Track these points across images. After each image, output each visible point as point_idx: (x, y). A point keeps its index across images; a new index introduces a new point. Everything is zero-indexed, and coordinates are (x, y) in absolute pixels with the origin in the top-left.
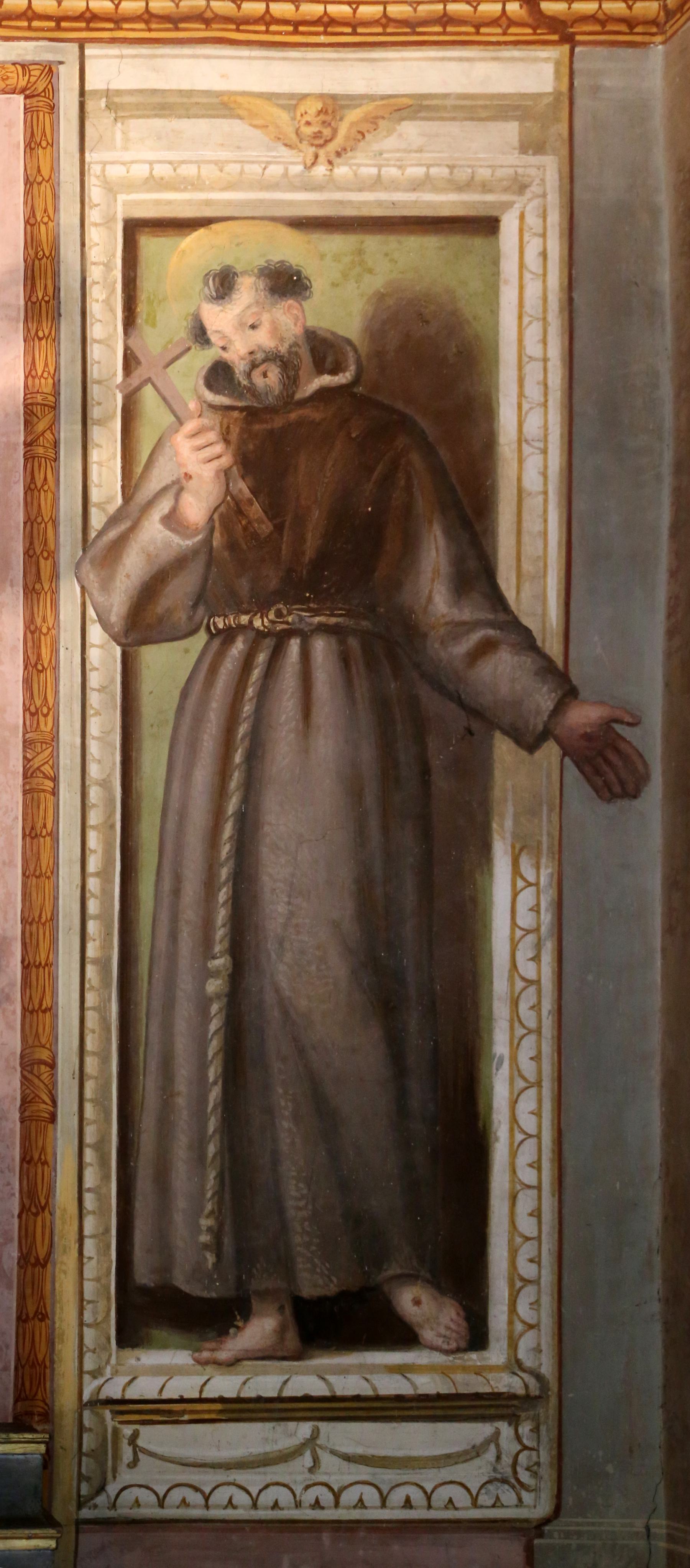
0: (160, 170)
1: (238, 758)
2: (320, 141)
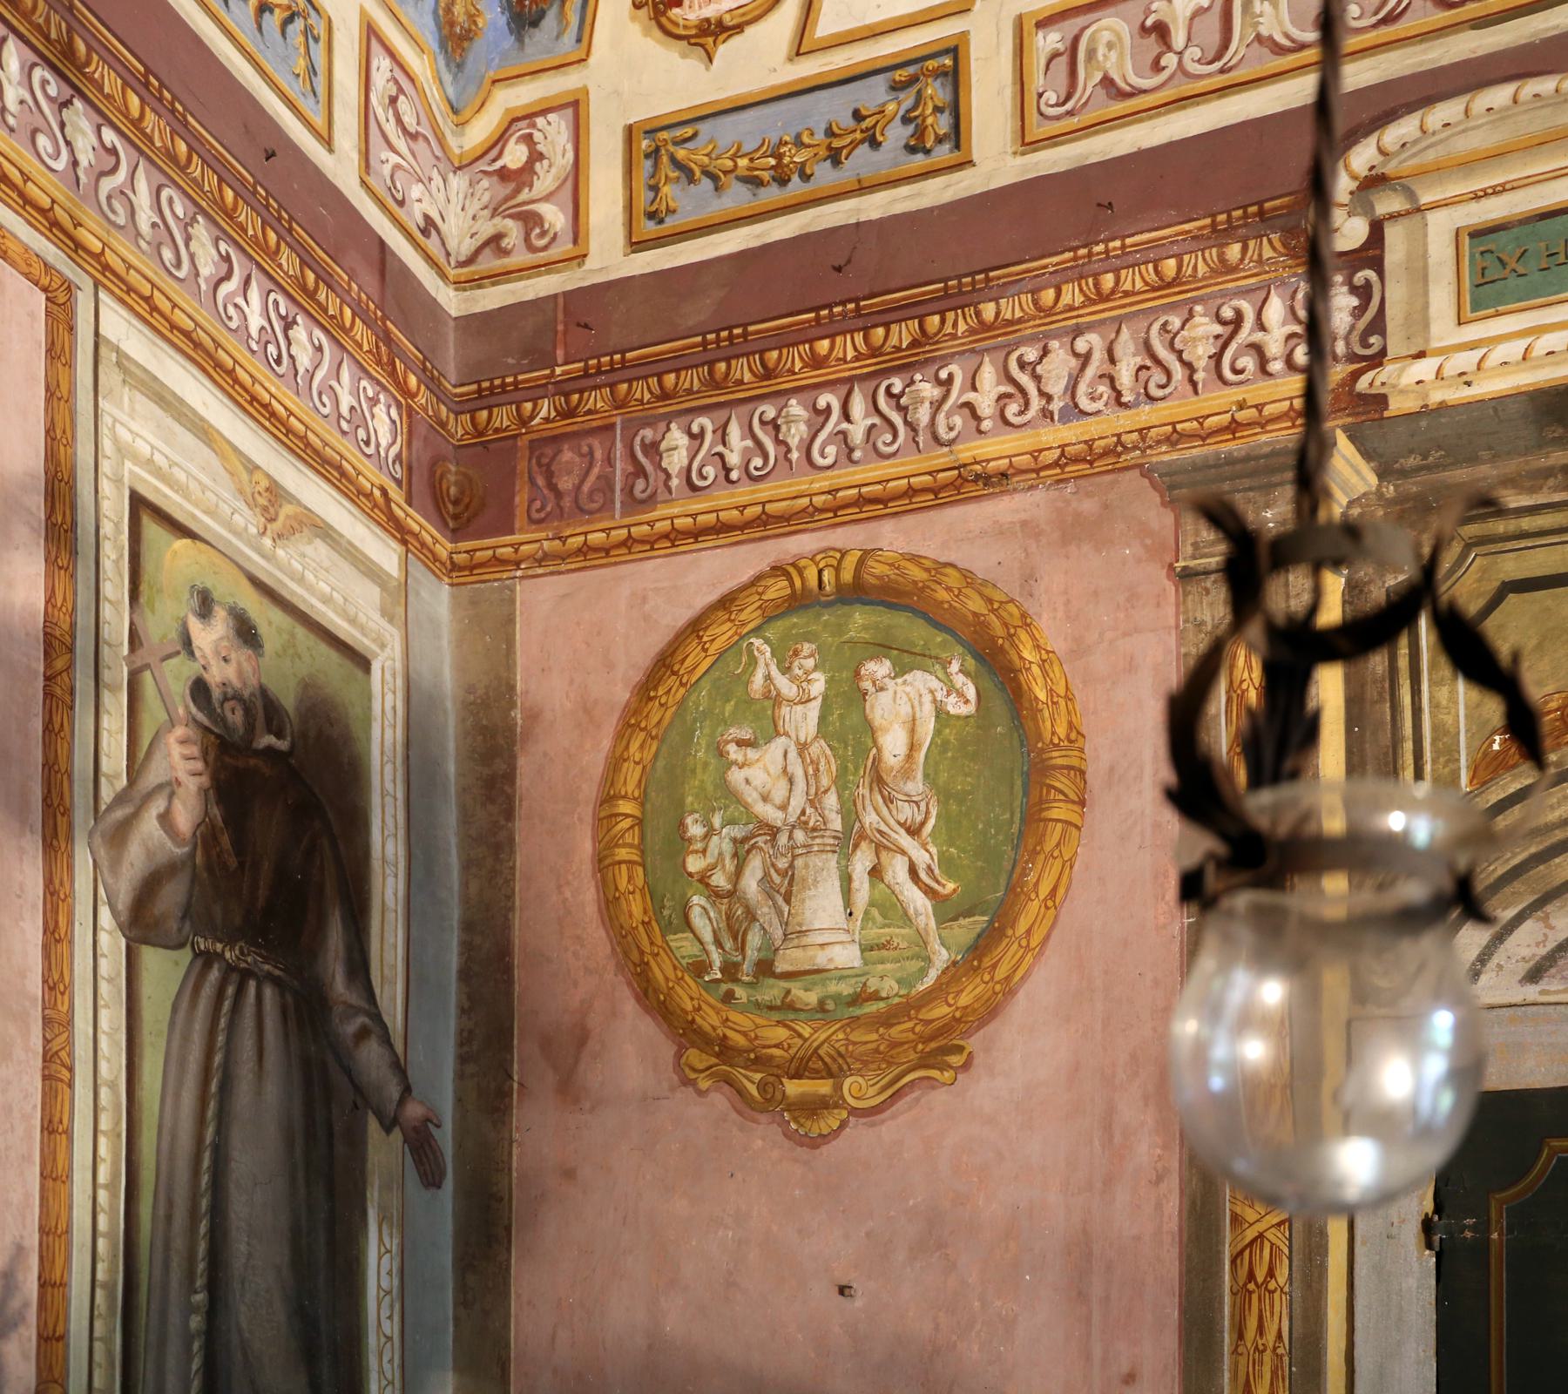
1: (214, 1087)
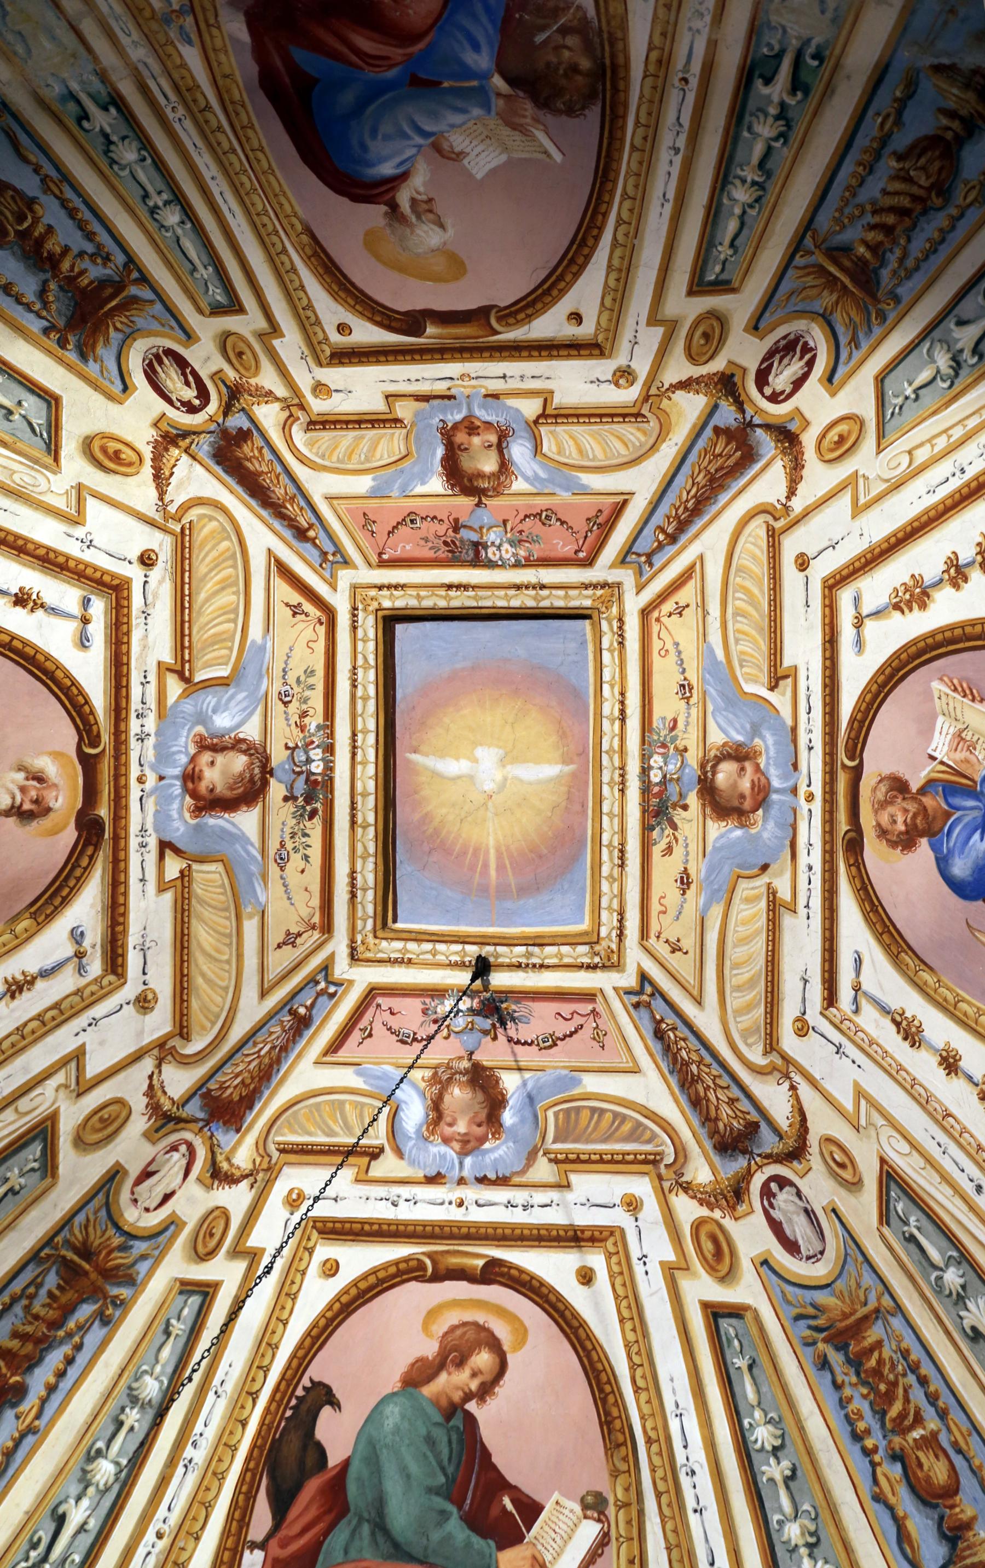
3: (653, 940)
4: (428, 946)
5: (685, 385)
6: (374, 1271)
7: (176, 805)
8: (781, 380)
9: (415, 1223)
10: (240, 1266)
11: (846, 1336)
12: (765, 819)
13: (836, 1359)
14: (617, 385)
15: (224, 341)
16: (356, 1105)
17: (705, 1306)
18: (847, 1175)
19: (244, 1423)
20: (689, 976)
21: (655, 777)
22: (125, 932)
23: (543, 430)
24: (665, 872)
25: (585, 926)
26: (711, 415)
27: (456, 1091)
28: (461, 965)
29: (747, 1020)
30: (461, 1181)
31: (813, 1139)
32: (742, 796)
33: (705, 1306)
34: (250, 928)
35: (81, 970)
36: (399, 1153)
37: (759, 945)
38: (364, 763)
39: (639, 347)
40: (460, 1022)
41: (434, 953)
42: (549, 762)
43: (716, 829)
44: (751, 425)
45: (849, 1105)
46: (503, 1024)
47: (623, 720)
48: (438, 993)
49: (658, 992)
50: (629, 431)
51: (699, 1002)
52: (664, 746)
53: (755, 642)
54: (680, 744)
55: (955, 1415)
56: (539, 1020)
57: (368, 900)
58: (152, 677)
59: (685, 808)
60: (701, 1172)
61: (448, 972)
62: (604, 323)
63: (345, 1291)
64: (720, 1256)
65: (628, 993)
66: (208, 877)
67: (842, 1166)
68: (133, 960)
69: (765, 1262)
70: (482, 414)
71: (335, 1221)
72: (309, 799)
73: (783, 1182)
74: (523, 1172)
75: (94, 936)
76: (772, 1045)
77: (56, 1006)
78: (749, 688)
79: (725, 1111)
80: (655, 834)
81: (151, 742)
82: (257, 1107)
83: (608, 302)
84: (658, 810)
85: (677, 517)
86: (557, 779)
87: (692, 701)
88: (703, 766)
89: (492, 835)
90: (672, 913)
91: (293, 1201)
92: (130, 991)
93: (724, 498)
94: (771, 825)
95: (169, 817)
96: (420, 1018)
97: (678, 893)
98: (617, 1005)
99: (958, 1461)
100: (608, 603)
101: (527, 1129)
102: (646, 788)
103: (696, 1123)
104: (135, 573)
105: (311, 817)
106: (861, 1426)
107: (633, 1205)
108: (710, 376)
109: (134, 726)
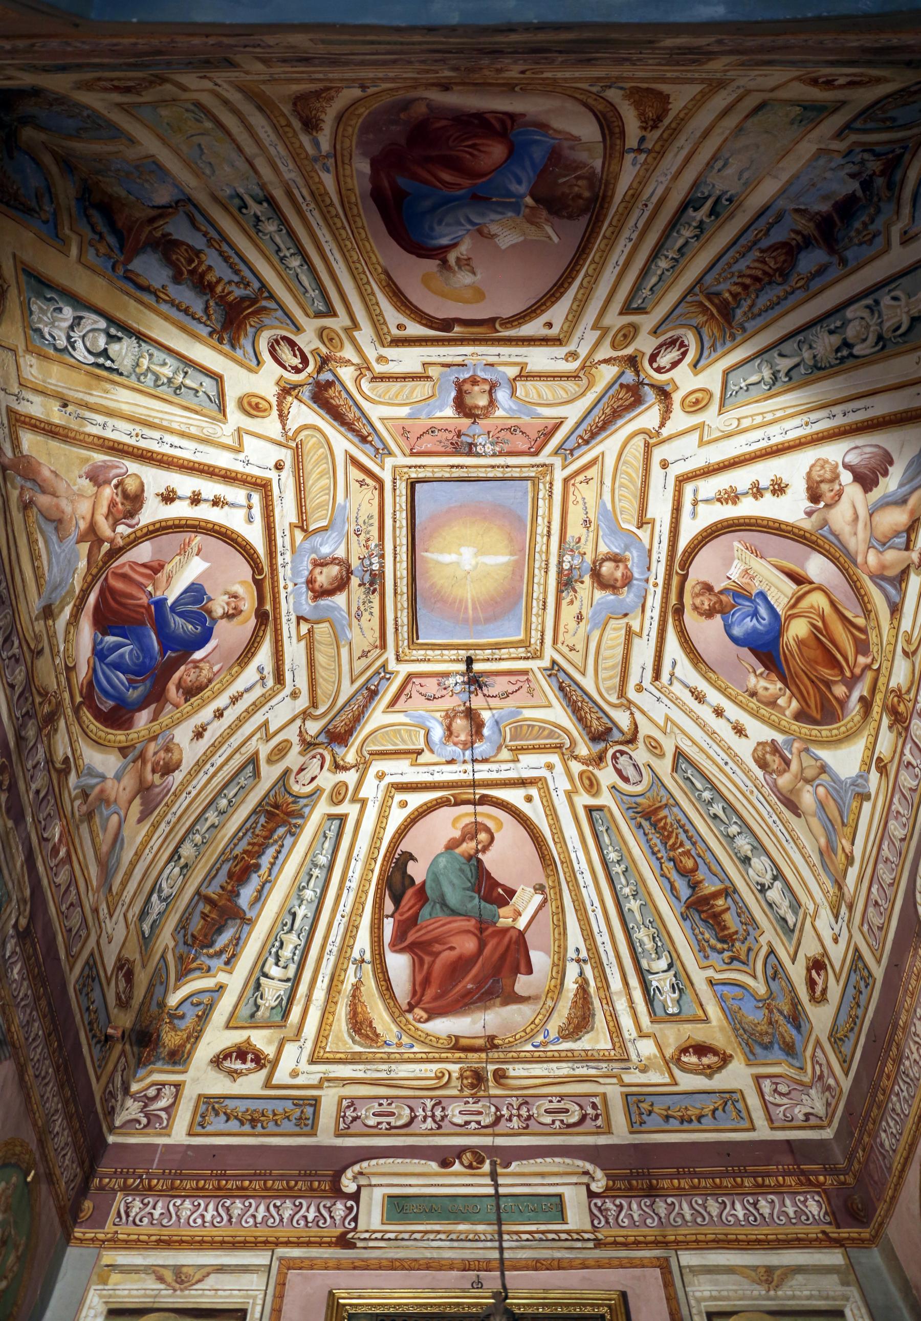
0: (714, 1293)
2: (769, 1282)
3: (559, 645)
4: (439, 652)
5: (606, 361)
6: (425, 804)
7: (304, 597)
8: (664, 360)
9: (444, 782)
10: (357, 806)
11: (651, 816)
12: (628, 592)
13: (646, 824)
14: (567, 360)
15: (321, 333)
16: (407, 731)
17: (586, 807)
18: (657, 751)
19: (372, 871)
20: (580, 664)
21: (566, 566)
22: (283, 663)
23: (518, 384)
24: (569, 614)
25: (522, 637)
26: (619, 377)
27: (459, 721)
28: (458, 661)
29: (609, 683)
30: (465, 762)
31: (640, 736)
32: (616, 580)
33: (586, 807)
34: (344, 652)
35: (264, 685)
36: (432, 751)
37: (620, 650)
38: (401, 562)
39: (584, 341)
40: (458, 688)
41: (442, 655)
42: (502, 554)
43: (599, 594)
44: (642, 383)
45: (661, 723)
46: (481, 688)
47: (549, 536)
48: (446, 675)
49: (561, 669)
50: (571, 386)
51: (584, 674)
52: (572, 551)
53: (631, 503)
54: (582, 551)
55: (700, 843)
56: (500, 685)
57: (404, 631)
58: (287, 532)
59: (582, 582)
60: (583, 750)
61: (450, 664)
62: (565, 328)
63: (413, 813)
64: (592, 786)
65: (545, 669)
66: (322, 630)
67: (655, 748)
68: (288, 676)
69: (614, 787)
70: (481, 374)
71: (402, 784)
72: (372, 583)
73: (622, 753)
74: (496, 756)
75: (269, 669)
76: (622, 694)
77: (254, 704)
78: (624, 526)
79: (595, 723)
80: (564, 594)
81: (289, 567)
82: (355, 735)
83: (570, 318)
84: (566, 582)
85: (591, 431)
86: (507, 564)
87: (591, 529)
88: (594, 563)
89: (469, 592)
90: (571, 632)
91: (381, 776)
92: (288, 690)
93: (620, 422)
94: (631, 595)
95: (301, 604)
96: (437, 687)
97: (575, 624)
98: (539, 676)
99: (699, 860)
100: (544, 475)
101: (496, 737)
102: (560, 572)
103: (580, 728)
104: (273, 475)
105: (373, 592)
106: (656, 849)
107: (550, 767)
108: (623, 357)
109: (280, 560)
